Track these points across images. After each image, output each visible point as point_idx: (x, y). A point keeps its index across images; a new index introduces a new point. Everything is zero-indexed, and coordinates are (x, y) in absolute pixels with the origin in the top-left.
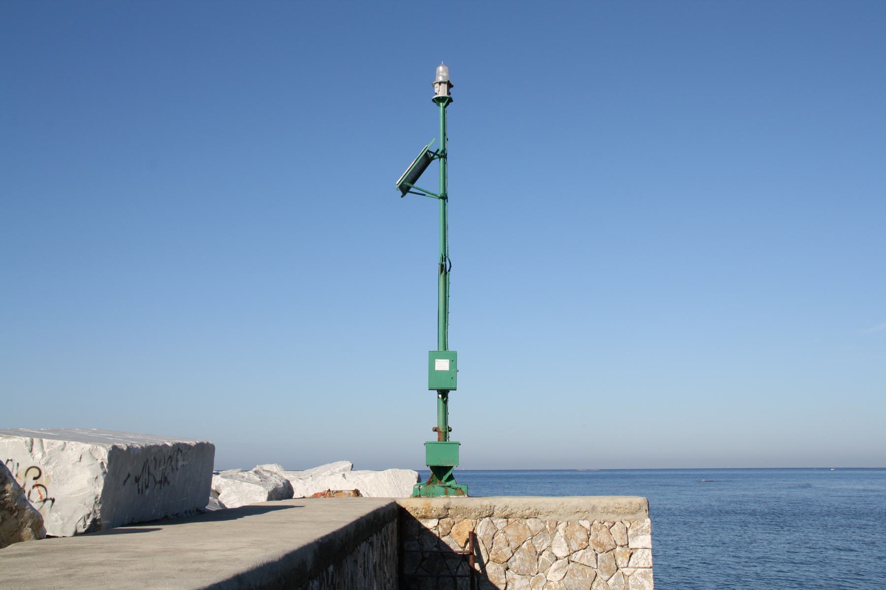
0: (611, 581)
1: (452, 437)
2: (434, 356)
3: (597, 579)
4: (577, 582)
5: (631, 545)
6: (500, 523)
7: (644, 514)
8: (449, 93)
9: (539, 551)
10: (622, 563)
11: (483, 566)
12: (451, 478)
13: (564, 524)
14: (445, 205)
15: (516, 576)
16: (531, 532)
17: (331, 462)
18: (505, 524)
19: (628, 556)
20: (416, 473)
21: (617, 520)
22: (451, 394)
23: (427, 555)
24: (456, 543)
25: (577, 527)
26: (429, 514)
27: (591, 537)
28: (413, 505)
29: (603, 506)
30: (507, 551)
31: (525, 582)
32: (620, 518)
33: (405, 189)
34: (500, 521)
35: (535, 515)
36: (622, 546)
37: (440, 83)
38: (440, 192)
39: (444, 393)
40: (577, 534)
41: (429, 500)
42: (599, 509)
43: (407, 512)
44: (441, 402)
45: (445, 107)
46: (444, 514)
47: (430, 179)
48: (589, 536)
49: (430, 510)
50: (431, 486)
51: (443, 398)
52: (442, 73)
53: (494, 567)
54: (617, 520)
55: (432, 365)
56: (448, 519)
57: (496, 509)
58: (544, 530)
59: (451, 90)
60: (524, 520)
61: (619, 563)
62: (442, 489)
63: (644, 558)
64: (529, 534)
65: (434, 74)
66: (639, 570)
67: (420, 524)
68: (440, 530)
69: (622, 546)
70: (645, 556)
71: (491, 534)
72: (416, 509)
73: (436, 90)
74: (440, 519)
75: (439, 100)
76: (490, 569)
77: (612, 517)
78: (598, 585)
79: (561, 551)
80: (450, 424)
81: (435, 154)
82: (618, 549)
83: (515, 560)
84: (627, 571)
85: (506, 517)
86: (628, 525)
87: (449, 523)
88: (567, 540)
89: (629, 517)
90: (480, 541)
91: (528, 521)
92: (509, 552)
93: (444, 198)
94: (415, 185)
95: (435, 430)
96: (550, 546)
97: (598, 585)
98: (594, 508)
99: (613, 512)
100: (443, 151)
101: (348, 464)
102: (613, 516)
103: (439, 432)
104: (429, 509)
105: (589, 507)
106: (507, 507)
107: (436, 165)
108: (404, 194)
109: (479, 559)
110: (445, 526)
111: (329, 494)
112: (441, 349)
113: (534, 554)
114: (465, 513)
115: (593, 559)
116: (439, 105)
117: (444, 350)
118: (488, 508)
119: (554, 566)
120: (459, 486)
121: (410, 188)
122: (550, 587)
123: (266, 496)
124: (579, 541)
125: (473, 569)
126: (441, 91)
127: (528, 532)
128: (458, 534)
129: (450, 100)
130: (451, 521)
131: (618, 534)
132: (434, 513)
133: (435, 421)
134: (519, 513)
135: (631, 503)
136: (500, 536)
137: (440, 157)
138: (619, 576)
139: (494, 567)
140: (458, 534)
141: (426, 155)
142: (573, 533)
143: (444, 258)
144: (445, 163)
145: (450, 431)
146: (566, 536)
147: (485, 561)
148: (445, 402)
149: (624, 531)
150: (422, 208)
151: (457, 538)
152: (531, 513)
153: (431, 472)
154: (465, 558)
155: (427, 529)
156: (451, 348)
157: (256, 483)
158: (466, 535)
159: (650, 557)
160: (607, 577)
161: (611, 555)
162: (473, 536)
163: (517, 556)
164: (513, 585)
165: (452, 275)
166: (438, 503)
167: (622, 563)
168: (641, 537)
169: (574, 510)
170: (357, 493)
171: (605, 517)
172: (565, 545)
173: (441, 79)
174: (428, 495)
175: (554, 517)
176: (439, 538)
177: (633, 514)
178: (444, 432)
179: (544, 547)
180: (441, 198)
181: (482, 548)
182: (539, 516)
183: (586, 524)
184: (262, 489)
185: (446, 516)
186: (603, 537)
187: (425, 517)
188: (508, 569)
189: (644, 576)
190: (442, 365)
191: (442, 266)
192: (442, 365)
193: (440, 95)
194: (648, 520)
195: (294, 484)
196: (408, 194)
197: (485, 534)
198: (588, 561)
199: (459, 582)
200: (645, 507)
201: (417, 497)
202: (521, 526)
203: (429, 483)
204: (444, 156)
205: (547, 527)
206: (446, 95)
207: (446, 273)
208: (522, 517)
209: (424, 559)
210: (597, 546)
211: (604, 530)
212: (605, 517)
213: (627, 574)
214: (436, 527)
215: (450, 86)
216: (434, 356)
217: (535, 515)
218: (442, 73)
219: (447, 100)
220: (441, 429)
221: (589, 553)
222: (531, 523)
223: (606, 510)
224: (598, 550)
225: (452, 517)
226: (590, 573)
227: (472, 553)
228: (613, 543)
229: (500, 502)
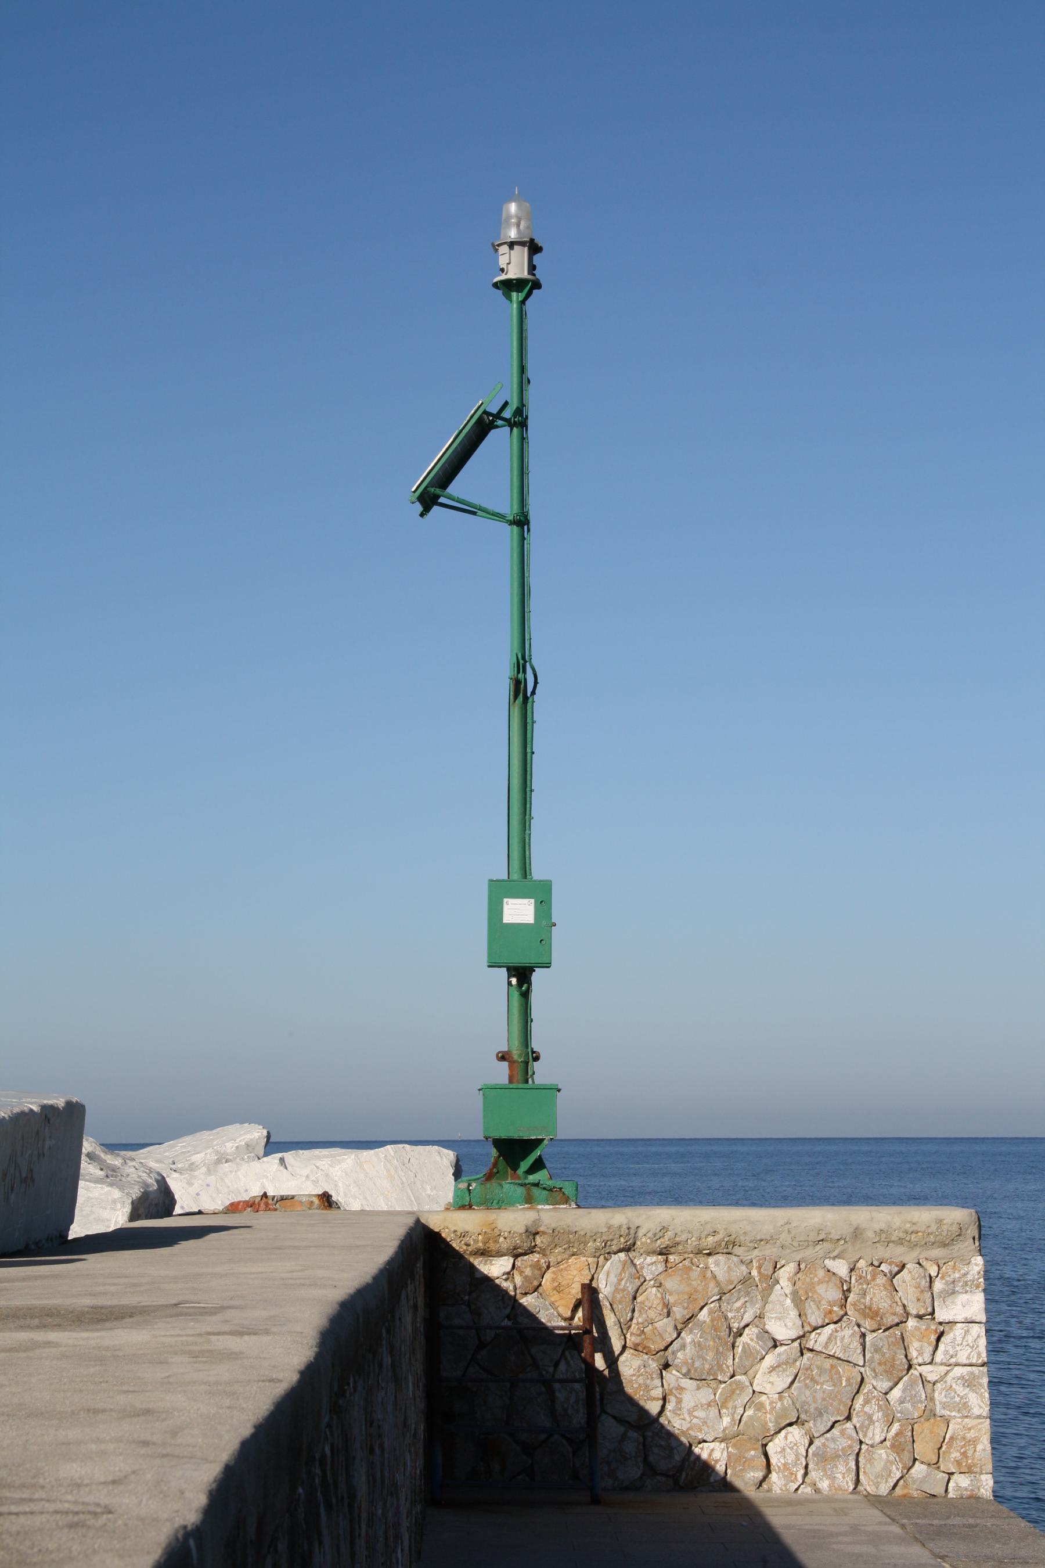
0: (896, 1394)
2: (499, 892)
3: (866, 1389)
4: (819, 1396)
5: (941, 1315)
6: (650, 1265)
7: (968, 1246)
8: (532, 268)
9: (735, 1326)
10: (921, 1353)
11: (612, 1361)
12: (538, 1165)
13: (790, 1268)
14: (523, 539)
15: (686, 1383)
17: (210, 1128)
18: (661, 1267)
19: (933, 1338)
20: (446, 1158)
21: (910, 1258)
23: (489, 1335)
24: (553, 1309)
25: (821, 1273)
26: (493, 1246)
28: (459, 1227)
29: (877, 1227)
30: (665, 1327)
31: (705, 1395)
32: (914, 1254)
33: (428, 500)
34: (650, 1259)
35: (728, 1247)
36: (920, 1317)
37: (511, 245)
38: (509, 508)
39: (522, 974)
40: (821, 1289)
41: (492, 1216)
42: (870, 1234)
43: (444, 1240)
44: (516, 995)
45: (523, 302)
46: (526, 1246)
49: (493, 1236)
50: (493, 1184)
51: (520, 984)
52: (514, 218)
53: (637, 1362)
54: (910, 1258)
55: (495, 911)
56: (535, 1257)
57: (640, 1234)
58: (746, 1280)
59: (537, 258)
61: (913, 1353)
62: (520, 1191)
63: (969, 1344)
64: (713, 1289)
65: (498, 221)
66: (958, 1371)
67: (472, 1267)
68: (518, 1280)
69: (920, 1317)
70: (970, 1339)
71: (631, 1289)
72: (464, 1235)
73: (503, 261)
74: (516, 1257)
75: (509, 286)
76: (629, 1366)
77: (899, 1253)
78: (867, 1402)
79: (784, 1328)
80: (536, 1044)
81: (498, 416)
82: (911, 1323)
83: (683, 1347)
84: (931, 1373)
85: (664, 1252)
87: (536, 1266)
88: (799, 1302)
89: (936, 1252)
90: (605, 1304)
92: (670, 1328)
93: (522, 522)
94: (452, 489)
95: (503, 1057)
96: (760, 1317)
97: (867, 1402)
98: (857, 1233)
99: (900, 1242)
100: (519, 411)
101: (257, 1134)
102: (900, 1250)
103: (512, 1063)
104: (492, 1234)
105: (847, 1231)
106: (664, 1229)
107: (500, 439)
108: (426, 510)
109: (603, 1343)
110: (528, 1272)
111: (264, 1203)
112: (516, 875)
113: (724, 1333)
114: (572, 1242)
115: (856, 1344)
116: (509, 298)
117: (521, 878)
119: (770, 1360)
120: (558, 1184)
121: (438, 497)
122: (760, 1407)
123: (128, 1209)
124: (825, 1306)
125: (590, 1366)
126: (514, 265)
127: (712, 1284)
128: (558, 1289)
129: (537, 285)
130: (543, 1259)
131: (911, 1290)
132: (504, 1244)
133: (500, 1035)
134: (693, 1242)
135: (940, 1222)
136: (651, 1295)
137: (511, 424)
138: (912, 1384)
139: (637, 1362)
140: (558, 1289)
141: (480, 420)
142: (811, 1287)
143: (522, 663)
144: (523, 439)
145: (536, 1059)
146: (795, 1295)
147: (617, 1347)
148: (526, 995)
149: (924, 1283)
150: (469, 548)
153: (494, 1152)
154: (572, 1342)
155: (487, 1280)
156: (537, 873)
157: (98, 1181)
158: (576, 1292)
159: (983, 1342)
160: (885, 1385)
161: (894, 1336)
162: (590, 1292)
163: (687, 1337)
164: (679, 1401)
166: (513, 1220)
167: (921, 1353)
168: (963, 1298)
169: (813, 1237)
170: (326, 1200)
171: (881, 1252)
172: (793, 1313)
173: (513, 234)
174: (488, 1203)
175: (770, 1251)
177: (945, 1245)
178: (522, 1061)
179: (747, 1318)
180: (512, 523)
181: (610, 1320)
182: (737, 1250)
183: (841, 1268)
184: (116, 1193)
185: (531, 1251)
186: (878, 1296)
187: (484, 1253)
188: (666, 1366)
189: (969, 1383)
190: (519, 911)
192: (519, 911)
193: (512, 274)
194: (979, 1260)
195: (175, 1185)
196: (435, 508)
197: (616, 1290)
198: (845, 1349)
199: (560, 1395)
200: (973, 1231)
201: (462, 1207)
202: (695, 1273)
203: (489, 1177)
204: (520, 422)
206: (525, 274)
208: (699, 1252)
209: (481, 1346)
210: (865, 1316)
211: (881, 1280)
212: (881, 1252)
213: (932, 1377)
215: (534, 248)
216: (499, 892)
217: (728, 1247)
218: (514, 218)
220: (516, 1055)
221: (848, 1332)
223: (884, 1237)
224: (868, 1324)
225: (543, 1252)
226: (847, 1375)
227: (588, 1332)
228: (899, 1310)
229: (651, 1219)
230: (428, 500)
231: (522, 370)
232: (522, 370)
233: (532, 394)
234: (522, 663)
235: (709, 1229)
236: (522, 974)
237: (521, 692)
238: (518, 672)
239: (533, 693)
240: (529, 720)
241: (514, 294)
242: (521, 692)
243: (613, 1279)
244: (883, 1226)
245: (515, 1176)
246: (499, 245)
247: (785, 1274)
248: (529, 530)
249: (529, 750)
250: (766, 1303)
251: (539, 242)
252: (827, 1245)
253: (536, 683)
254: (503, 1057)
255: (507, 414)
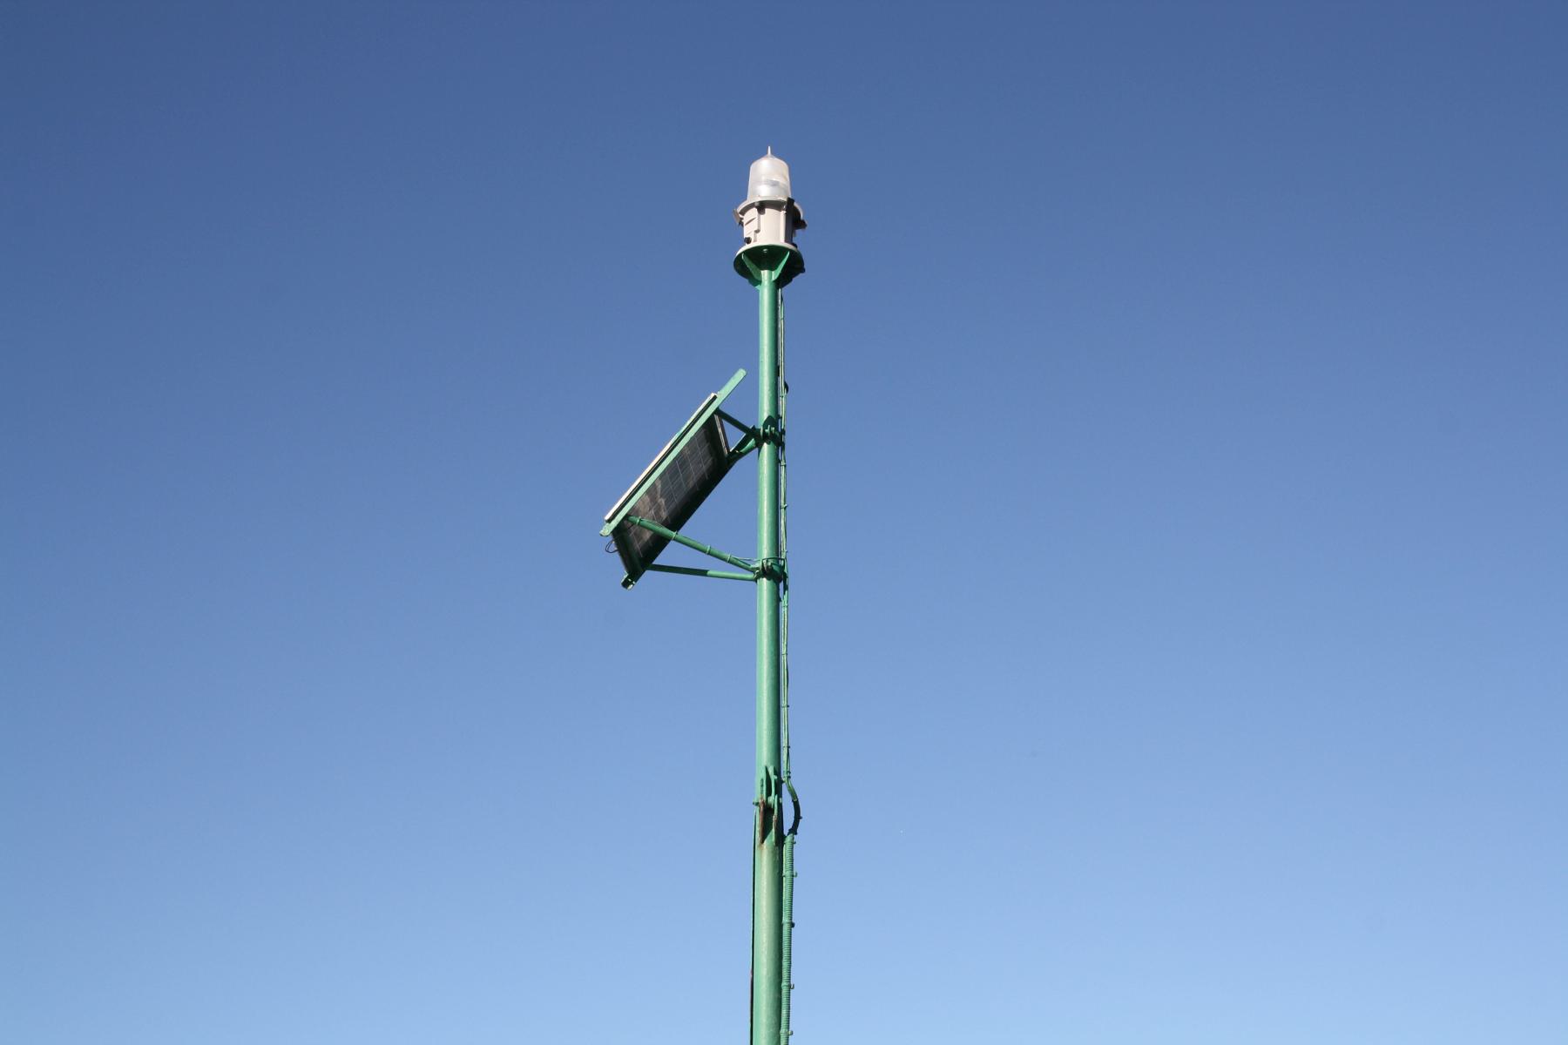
37: (762, 207)
45: (779, 283)
52: (768, 176)
73: (748, 231)
100: (773, 420)
116: (757, 282)
126: (767, 230)
129: (795, 266)
143: (775, 784)
165: (803, 847)
180: (766, 572)
191: (767, 810)
193: (761, 240)
196: (648, 574)
206: (780, 241)
207: (780, 840)
215: (794, 222)
218: (768, 176)
219: (788, 264)
230: (638, 553)
237: (774, 824)
238: (769, 794)
239: (794, 830)
240: (786, 872)
241: (765, 274)
242: (774, 824)
246: (743, 212)
248: (786, 588)
249: (785, 920)
253: (797, 817)
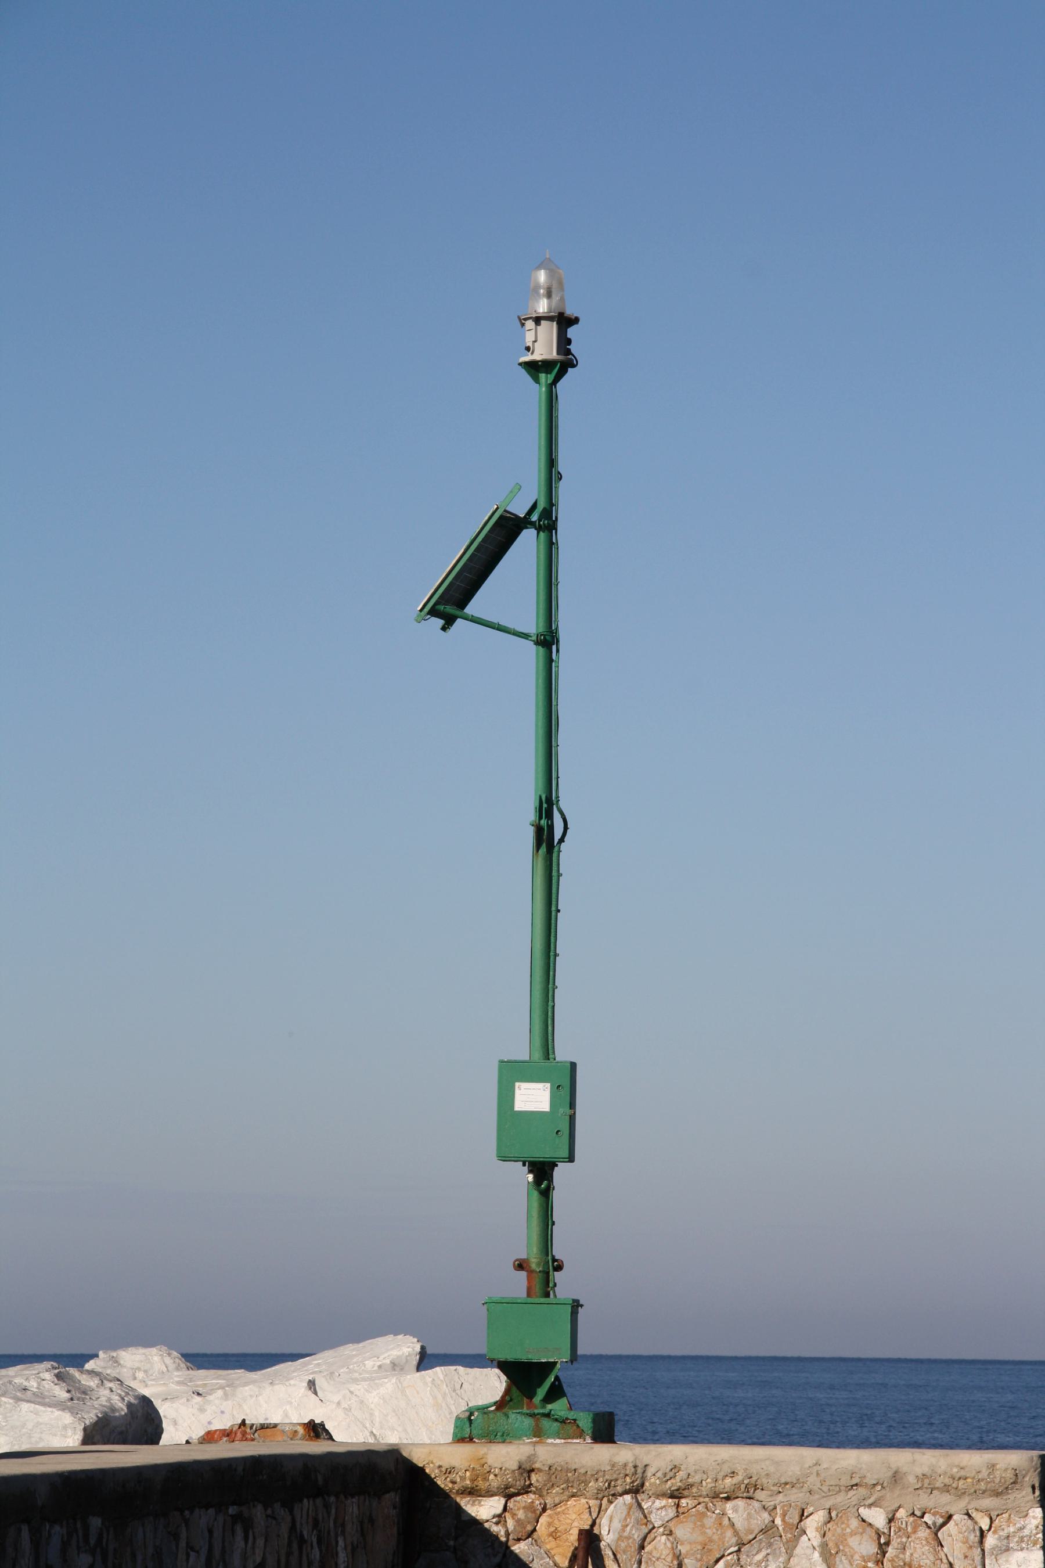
1: (565, 1285)
6: (660, 1510)
7: (1026, 1497)
12: (556, 1392)
13: (820, 1517)
14: (549, 661)
16: (736, 1533)
18: (671, 1513)
21: (957, 1507)
22: (561, 1173)
25: (854, 1523)
26: (482, 1485)
27: (891, 1551)
29: (919, 1471)
32: (962, 1504)
34: (659, 1503)
35: (748, 1490)
37: (538, 320)
40: (853, 1542)
43: (428, 1477)
44: (535, 1194)
46: (519, 1484)
47: (511, 588)
48: (883, 1548)
51: (538, 1182)
54: (957, 1507)
55: (506, 1096)
56: (529, 1498)
57: (650, 1472)
58: (769, 1529)
59: (572, 332)
60: (719, 1504)
62: (528, 1422)
64: (730, 1538)
67: (458, 1507)
68: (511, 1524)
71: (637, 1536)
72: (449, 1471)
73: (529, 338)
74: (509, 1497)
75: (534, 368)
77: (943, 1501)
80: (558, 1252)
85: (676, 1495)
86: (985, 1524)
87: (530, 1508)
89: (988, 1502)
90: (607, 1553)
91: (729, 1505)
93: (548, 641)
95: (520, 1266)
98: (896, 1477)
99: (946, 1489)
102: (945, 1498)
103: (530, 1272)
104: (482, 1471)
105: (885, 1475)
106: (676, 1469)
110: (521, 1514)
112: (538, 1055)
114: (572, 1482)
118: (630, 1470)
120: (571, 1415)
127: (729, 1533)
128: (554, 1535)
131: (958, 1545)
132: (494, 1482)
134: (708, 1484)
136: (660, 1545)
140: (554, 1535)
142: (842, 1539)
143: (547, 806)
145: (559, 1268)
146: (824, 1546)
148: (546, 1194)
149: (974, 1538)
151: (550, 1544)
152: (737, 1486)
156: (563, 1053)
165: (567, 855)
168: (1019, 1556)
169: (846, 1481)
171: (924, 1500)
175: (796, 1496)
176: (506, 1546)
177: (997, 1494)
178: (543, 1272)
182: (759, 1495)
183: (877, 1518)
184: (67, 1418)
185: (525, 1490)
187: (472, 1492)
190: (534, 1097)
191: (539, 830)
192: (534, 1097)
194: (1038, 1512)
197: (620, 1538)
202: (710, 1520)
204: (548, 524)
205: (778, 1521)
206: (553, 355)
207: (550, 847)
208: (715, 1496)
211: (923, 1533)
212: (924, 1500)
214: (500, 1518)
216: (512, 1073)
217: (748, 1490)
222: (737, 1511)
223: (928, 1484)
225: (539, 1493)
229: (660, 1458)
231: (551, 462)
232: (551, 462)
233: (564, 491)
234: (547, 806)
235: (726, 1469)
236: (542, 1172)
237: (546, 840)
238: (540, 818)
239: (562, 840)
240: (554, 873)
241: (542, 376)
242: (546, 840)
243: (617, 1525)
244: (926, 1470)
245: (530, 1405)
246: (526, 319)
247: (813, 1523)
248: (558, 651)
249: (553, 908)
250: (790, 1555)
251: (570, 311)
252: (862, 1491)
253: (566, 828)
254: (520, 1266)
255: (534, 517)
